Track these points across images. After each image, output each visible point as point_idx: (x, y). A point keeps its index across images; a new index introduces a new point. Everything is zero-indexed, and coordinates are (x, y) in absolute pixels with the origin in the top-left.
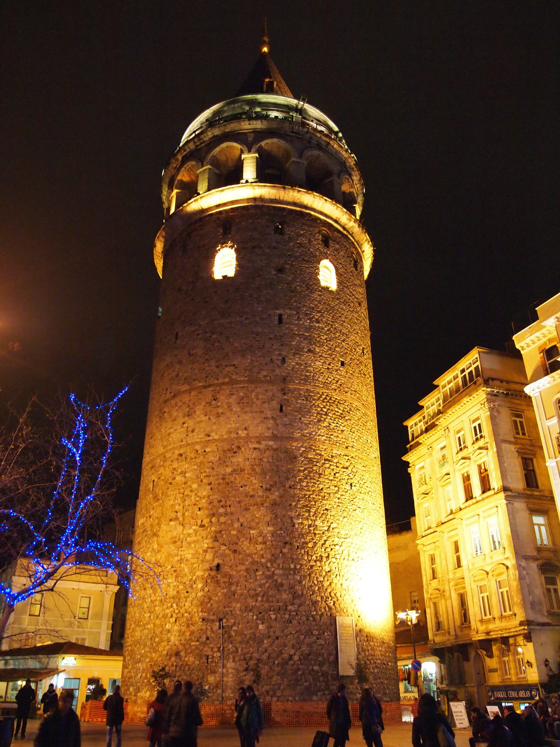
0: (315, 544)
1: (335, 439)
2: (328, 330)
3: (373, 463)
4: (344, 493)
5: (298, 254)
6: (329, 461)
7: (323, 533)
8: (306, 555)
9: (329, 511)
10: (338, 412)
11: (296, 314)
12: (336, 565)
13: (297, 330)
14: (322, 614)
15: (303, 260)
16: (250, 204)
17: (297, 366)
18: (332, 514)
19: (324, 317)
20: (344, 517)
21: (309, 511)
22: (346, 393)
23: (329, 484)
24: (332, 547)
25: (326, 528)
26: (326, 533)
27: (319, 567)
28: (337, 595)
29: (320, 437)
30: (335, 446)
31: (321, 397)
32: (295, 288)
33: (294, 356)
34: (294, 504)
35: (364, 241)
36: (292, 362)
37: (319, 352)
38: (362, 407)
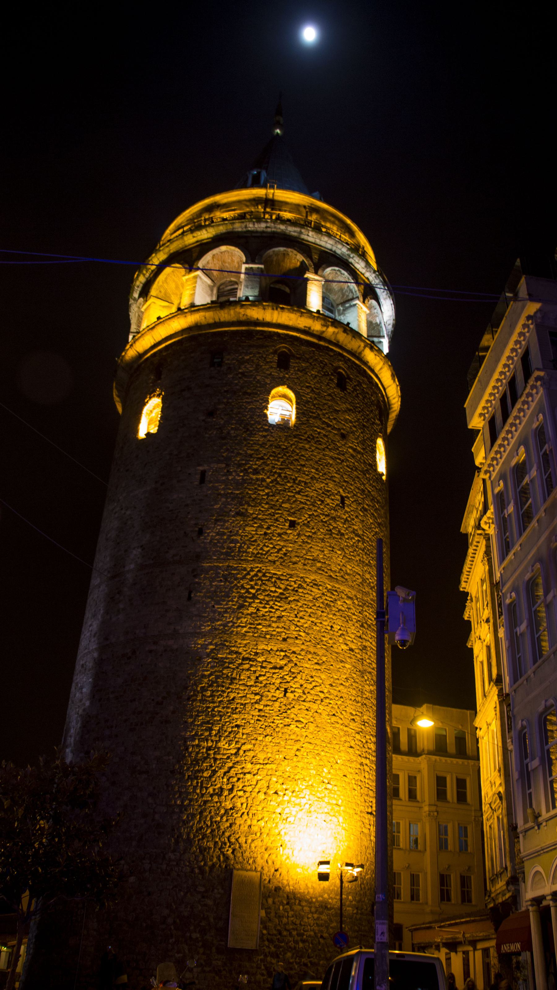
0: (214, 772)
1: (264, 629)
2: (272, 482)
3: (341, 657)
4: (270, 703)
5: (238, 387)
6: (250, 660)
7: (228, 758)
8: (199, 788)
9: (241, 728)
10: (275, 592)
11: (225, 468)
12: (243, 800)
13: (223, 489)
14: (214, 865)
15: (245, 393)
16: (184, 336)
17: (217, 537)
18: (245, 731)
19: (268, 465)
20: (266, 736)
21: (211, 729)
22: (295, 563)
23: (246, 692)
24: (239, 776)
25: (234, 751)
26: (233, 758)
27: (217, 802)
28: (240, 840)
29: (239, 629)
30: (262, 639)
31: (248, 574)
32: (228, 433)
33: (215, 524)
34: (190, 720)
35: (362, 348)
36: (211, 534)
37: (253, 514)
38: (326, 581)
